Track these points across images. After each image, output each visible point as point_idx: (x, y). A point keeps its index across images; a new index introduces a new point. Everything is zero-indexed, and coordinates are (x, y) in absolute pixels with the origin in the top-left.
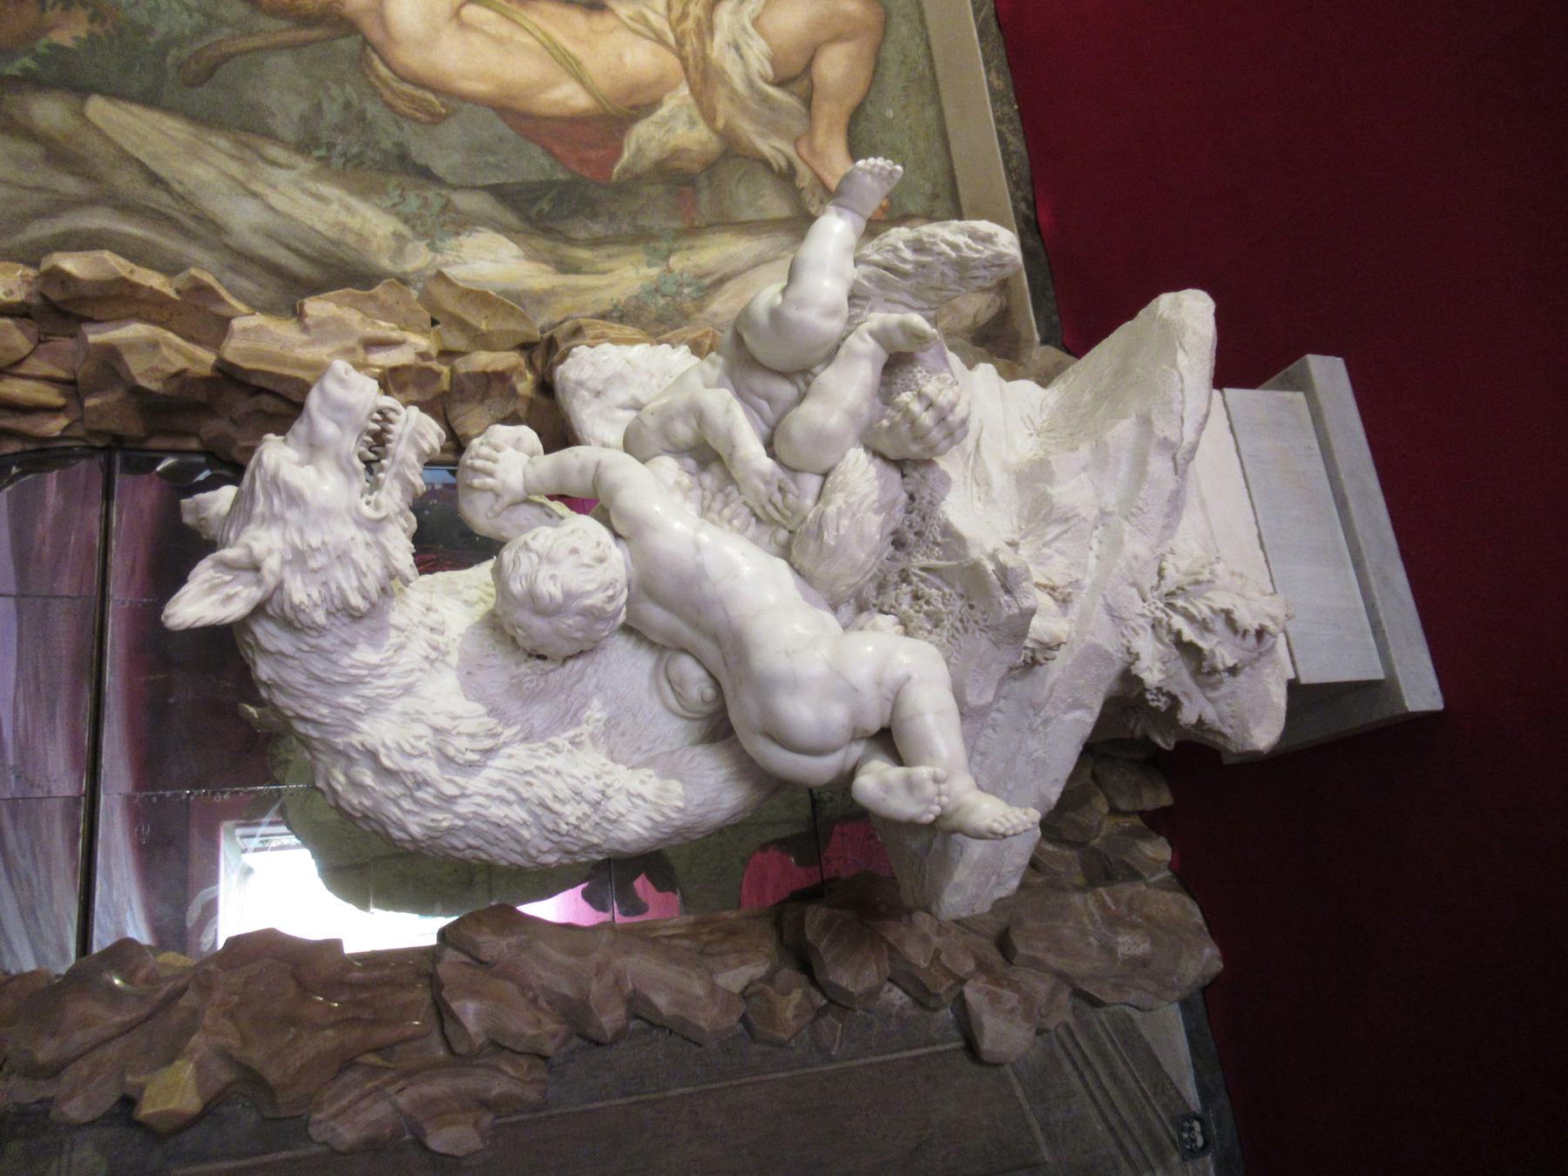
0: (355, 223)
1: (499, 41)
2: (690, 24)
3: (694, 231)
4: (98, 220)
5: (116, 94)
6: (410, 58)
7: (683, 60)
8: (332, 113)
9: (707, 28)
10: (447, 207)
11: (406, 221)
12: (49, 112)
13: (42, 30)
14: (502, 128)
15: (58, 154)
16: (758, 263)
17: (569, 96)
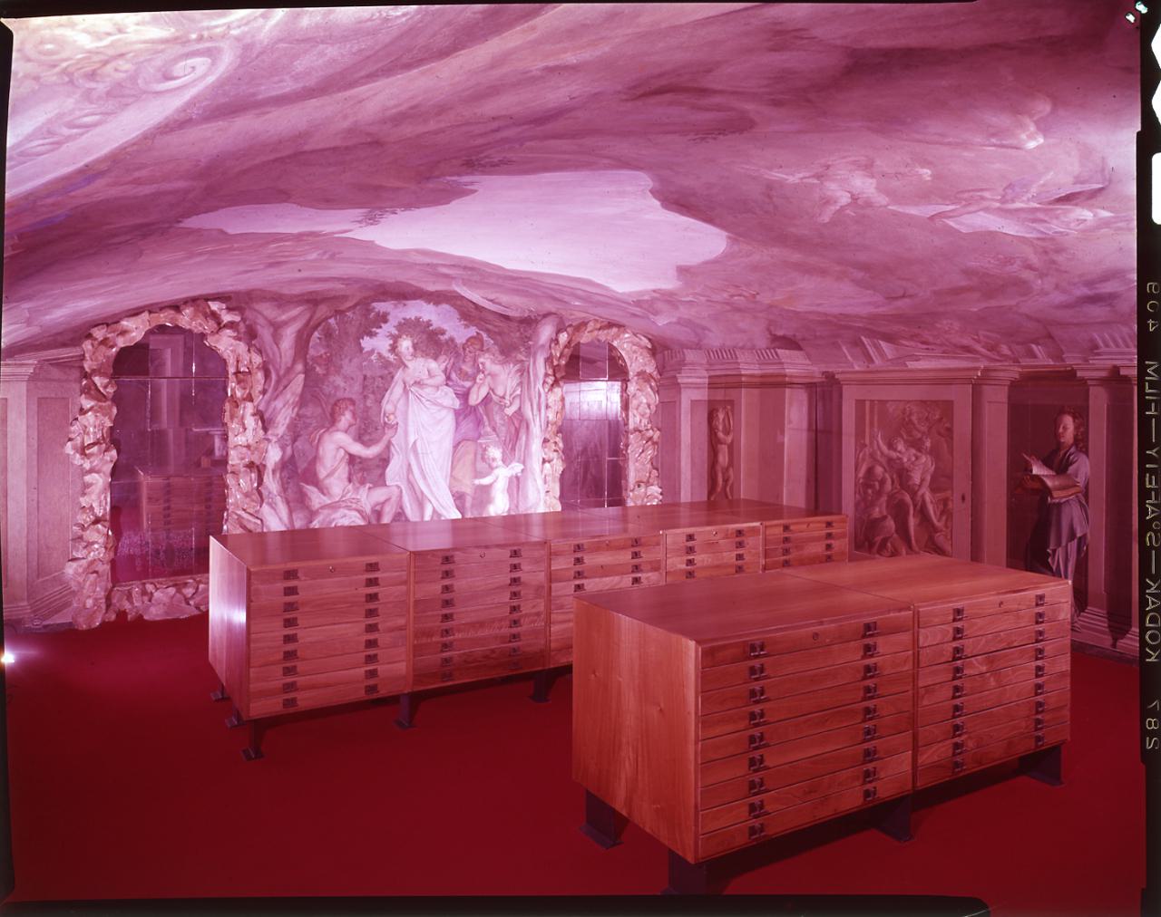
0: (280, 425)
1: (335, 457)
2: (349, 504)
3: (288, 503)
4: (274, 376)
5: (305, 379)
6: (326, 437)
7: (338, 502)
8: (308, 421)
9: (349, 508)
10: (287, 445)
11: (282, 437)
12: (299, 367)
13: (320, 365)
14: (310, 458)
15: (289, 370)
16: (280, 519)
17: (322, 473)
